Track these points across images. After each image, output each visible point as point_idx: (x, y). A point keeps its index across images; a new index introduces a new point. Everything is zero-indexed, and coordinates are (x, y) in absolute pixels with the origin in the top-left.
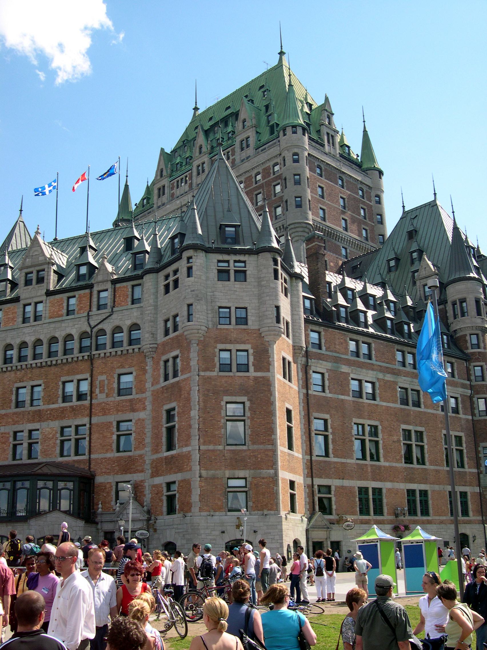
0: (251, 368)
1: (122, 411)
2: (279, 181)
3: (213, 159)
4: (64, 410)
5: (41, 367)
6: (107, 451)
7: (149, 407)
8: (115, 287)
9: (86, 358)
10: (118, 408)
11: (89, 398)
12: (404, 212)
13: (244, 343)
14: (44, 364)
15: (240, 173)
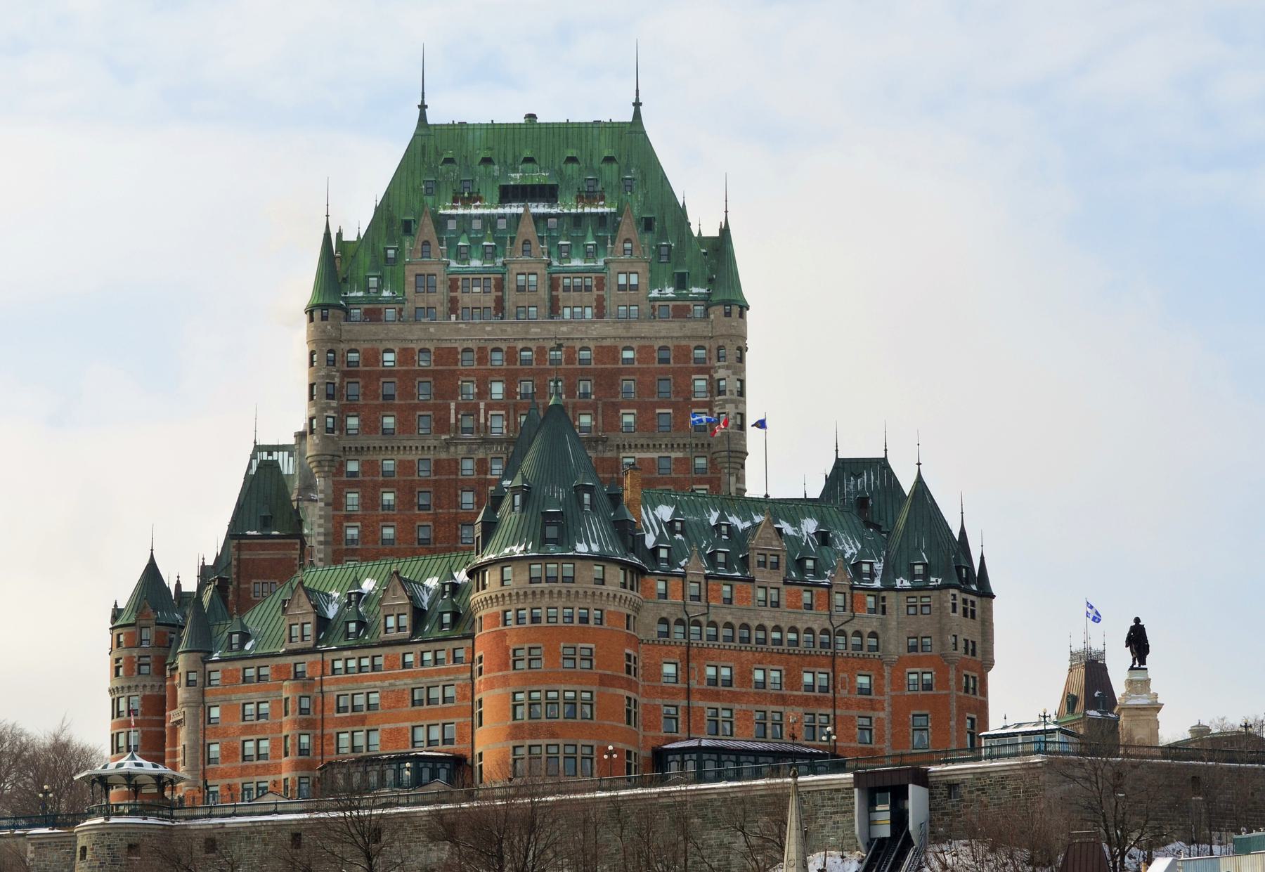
0: (978, 693)
1: (864, 708)
2: (707, 377)
3: (554, 276)
4: (807, 699)
5: (782, 653)
6: (851, 741)
7: (888, 709)
8: (852, 594)
9: (829, 654)
10: (860, 705)
11: (831, 691)
12: (837, 460)
13: (975, 671)
14: (786, 651)
15: (630, 335)
